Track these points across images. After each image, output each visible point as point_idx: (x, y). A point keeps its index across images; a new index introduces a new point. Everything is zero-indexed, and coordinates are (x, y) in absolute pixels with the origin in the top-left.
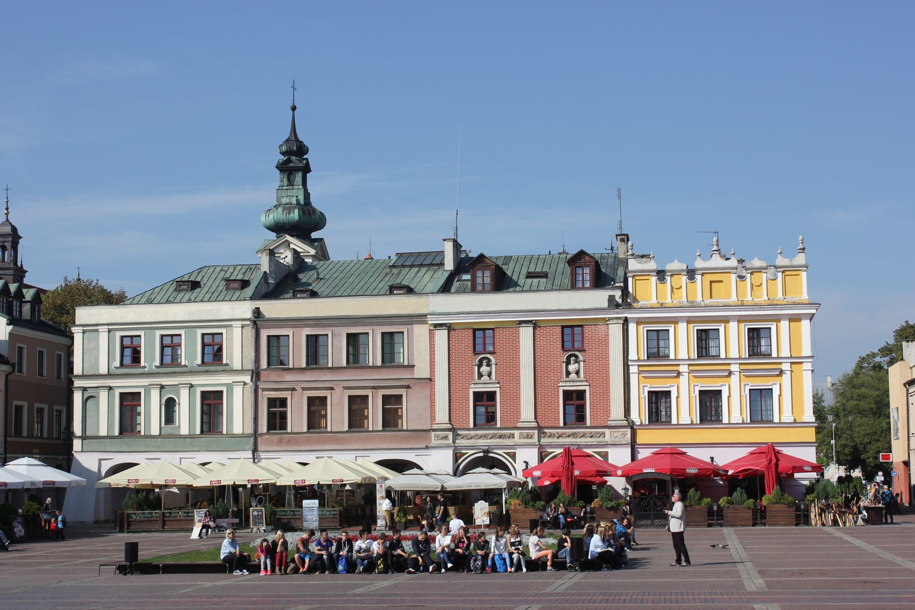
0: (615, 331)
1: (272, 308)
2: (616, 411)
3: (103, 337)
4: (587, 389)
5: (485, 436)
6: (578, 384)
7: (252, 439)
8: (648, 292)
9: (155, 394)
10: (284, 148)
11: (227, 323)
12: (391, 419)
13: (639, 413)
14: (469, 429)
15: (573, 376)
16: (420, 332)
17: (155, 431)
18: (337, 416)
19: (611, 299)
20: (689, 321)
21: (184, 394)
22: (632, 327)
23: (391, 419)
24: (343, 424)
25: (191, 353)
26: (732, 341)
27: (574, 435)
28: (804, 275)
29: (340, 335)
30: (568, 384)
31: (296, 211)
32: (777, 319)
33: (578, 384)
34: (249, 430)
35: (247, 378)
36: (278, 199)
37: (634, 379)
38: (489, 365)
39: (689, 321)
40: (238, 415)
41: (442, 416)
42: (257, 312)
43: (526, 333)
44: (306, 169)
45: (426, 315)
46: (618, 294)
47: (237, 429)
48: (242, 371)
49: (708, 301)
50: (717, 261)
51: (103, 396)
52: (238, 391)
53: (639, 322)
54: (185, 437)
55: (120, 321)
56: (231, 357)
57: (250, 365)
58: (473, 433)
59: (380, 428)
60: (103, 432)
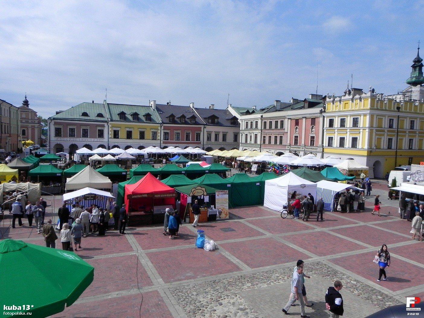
0: (321, 119)
1: (265, 115)
2: (320, 143)
3: (244, 122)
4: (298, 135)
9: (249, 134)
13: (326, 143)
17: (249, 143)
20: (339, 116)
21: (252, 134)
22: (325, 119)
26: (349, 122)
27: (312, 149)
35: (260, 132)
36: (411, 76)
37: (325, 133)
39: (339, 116)
41: (288, 142)
42: (262, 116)
43: (304, 120)
44: (422, 65)
47: (259, 143)
49: (344, 110)
52: (259, 134)
53: (328, 117)
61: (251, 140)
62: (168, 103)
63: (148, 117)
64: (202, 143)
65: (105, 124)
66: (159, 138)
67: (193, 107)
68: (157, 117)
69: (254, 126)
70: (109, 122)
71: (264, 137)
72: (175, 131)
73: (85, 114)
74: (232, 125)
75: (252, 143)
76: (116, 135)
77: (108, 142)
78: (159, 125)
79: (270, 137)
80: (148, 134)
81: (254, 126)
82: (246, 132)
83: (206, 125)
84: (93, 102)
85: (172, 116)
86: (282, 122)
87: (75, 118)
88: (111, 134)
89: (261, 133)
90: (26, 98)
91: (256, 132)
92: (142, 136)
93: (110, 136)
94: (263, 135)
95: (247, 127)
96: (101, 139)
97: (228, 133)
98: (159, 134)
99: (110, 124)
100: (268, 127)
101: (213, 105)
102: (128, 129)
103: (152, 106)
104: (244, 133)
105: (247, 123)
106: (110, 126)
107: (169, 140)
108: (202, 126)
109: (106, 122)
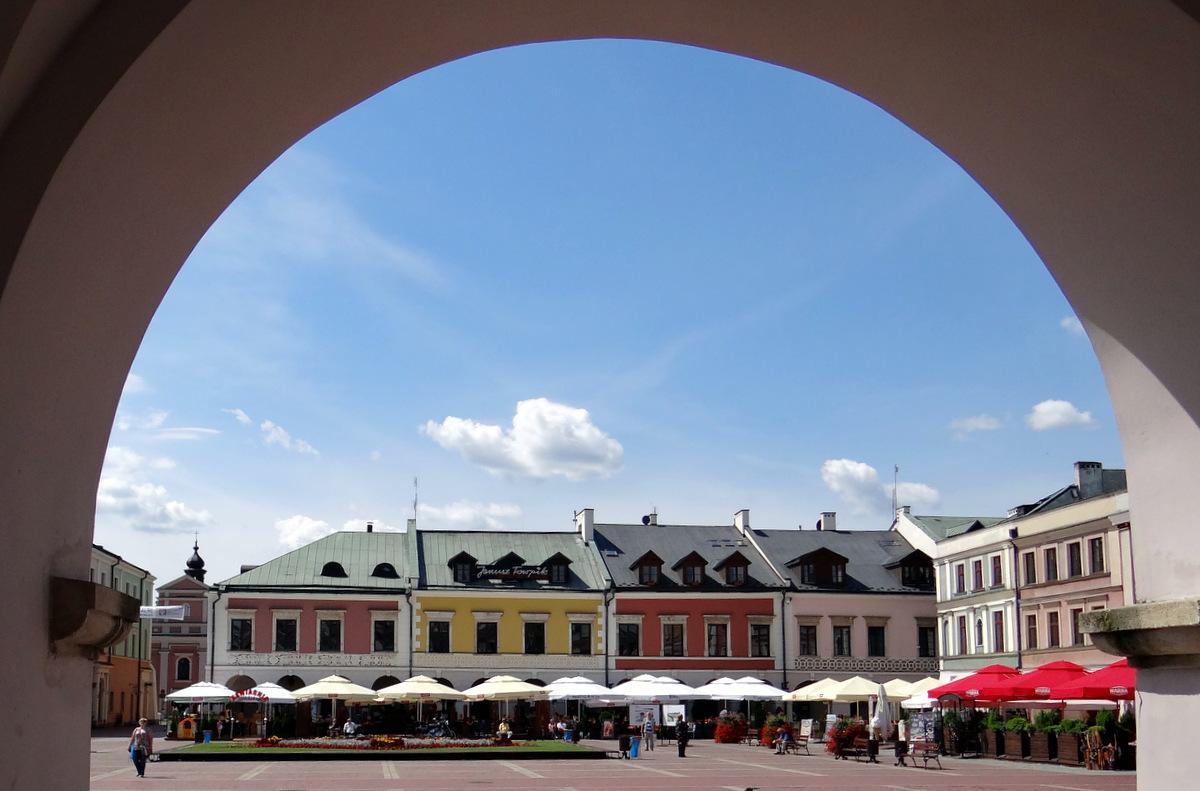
3: (948, 566)
7: (1017, 658)
9: (971, 615)
17: (973, 652)
21: (984, 613)
34: (1017, 649)
35: (1014, 599)
42: (1014, 533)
52: (1009, 609)
57: (1014, 587)
60: (951, 654)
61: (981, 641)
62: (646, 519)
63: (558, 570)
64: (778, 665)
65: (401, 599)
66: (601, 647)
67: (746, 526)
68: (591, 569)
69: (988, 580)
70: (413, 592)
71: (1032, 619)
72: (665, 620)
73: (333, 570)
74: (907, 589)
75: (986, 651)
76: (439, 640)
77: (411, 666)
78: (600, 596)
79: (1053, 617)
80: (558, 635)
81: (988, 580)
82: (961, 610)
83: (793, 589)
84: (370, 528)
85: (650, 560)
86: (1096, 547)
87: (297, 584)
88: (422, 635)
89: (1018, 605)
90: (196, 553)
91: (997, 603)
92: (535, 640)
93: (417, 645)
94: (1024, 615)
95: (961, 588)
96: (384, 658)
97: (889, 622)
98: (601, 634)
99: (419, 599)
100: (1041, 576)
101: (830, 515)
102: (481, 617)
103: (580, 533)
104: (952, 613)
105: (961, 567)
106: (417, 606)
107: (641, 653)
108: (776, 596)
109: (401, 591)
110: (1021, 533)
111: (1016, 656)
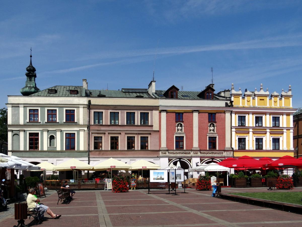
1: (95, 101)
3: (21, 110)
5: (180, 153)
6: (214, 134)
7: (87, 153)
8: (239, 102)
9: (45, 134)
10: (28, 68)
11: (77, 106)
12: (144, 147)
13: (235, 146)
14: (174, 150)
15: (212, 131)
16: (156, 113)
17: (45, 148)
18: (122, 144)
19: (226, 104)
23: (144, 147)
24: (125, 148)
25: (61, 117)
26: (267, 121)
27: (212, 153)
28: (291, 99)
29: (124, 113)
30: (210, 134)
31: (33, 89)
32: (282, 114)
33: (214, 134)
35: (86, 129)
36: (27, 85)
37: (234, 133)
38: (181, 126)
40: (82, 143)
41: (164, 145)
42: (90, 102)
45: (159, 106)
46: (229, 102)
47: (82, 148)
48: (83, 126)
50: (262, 92)
51: (22, 134)
52: (82, 134)
54: (58, 152)
55: (29, 103)
56: (78, 119)
57: (87, 123)
58: (175, 152)
59: (140, 149)
60: (22, 148)
75: (59, 149)
110: (92, 103)
111: (88, 152)
